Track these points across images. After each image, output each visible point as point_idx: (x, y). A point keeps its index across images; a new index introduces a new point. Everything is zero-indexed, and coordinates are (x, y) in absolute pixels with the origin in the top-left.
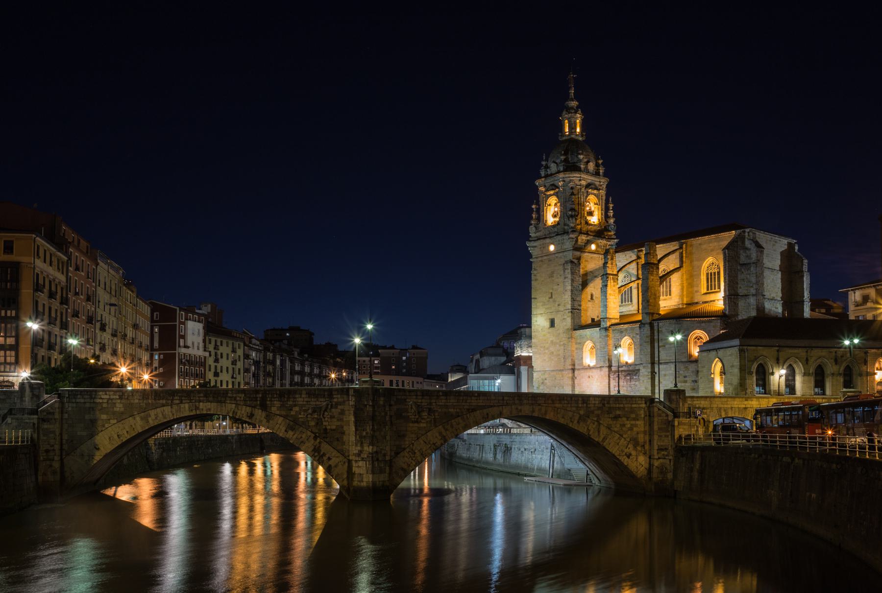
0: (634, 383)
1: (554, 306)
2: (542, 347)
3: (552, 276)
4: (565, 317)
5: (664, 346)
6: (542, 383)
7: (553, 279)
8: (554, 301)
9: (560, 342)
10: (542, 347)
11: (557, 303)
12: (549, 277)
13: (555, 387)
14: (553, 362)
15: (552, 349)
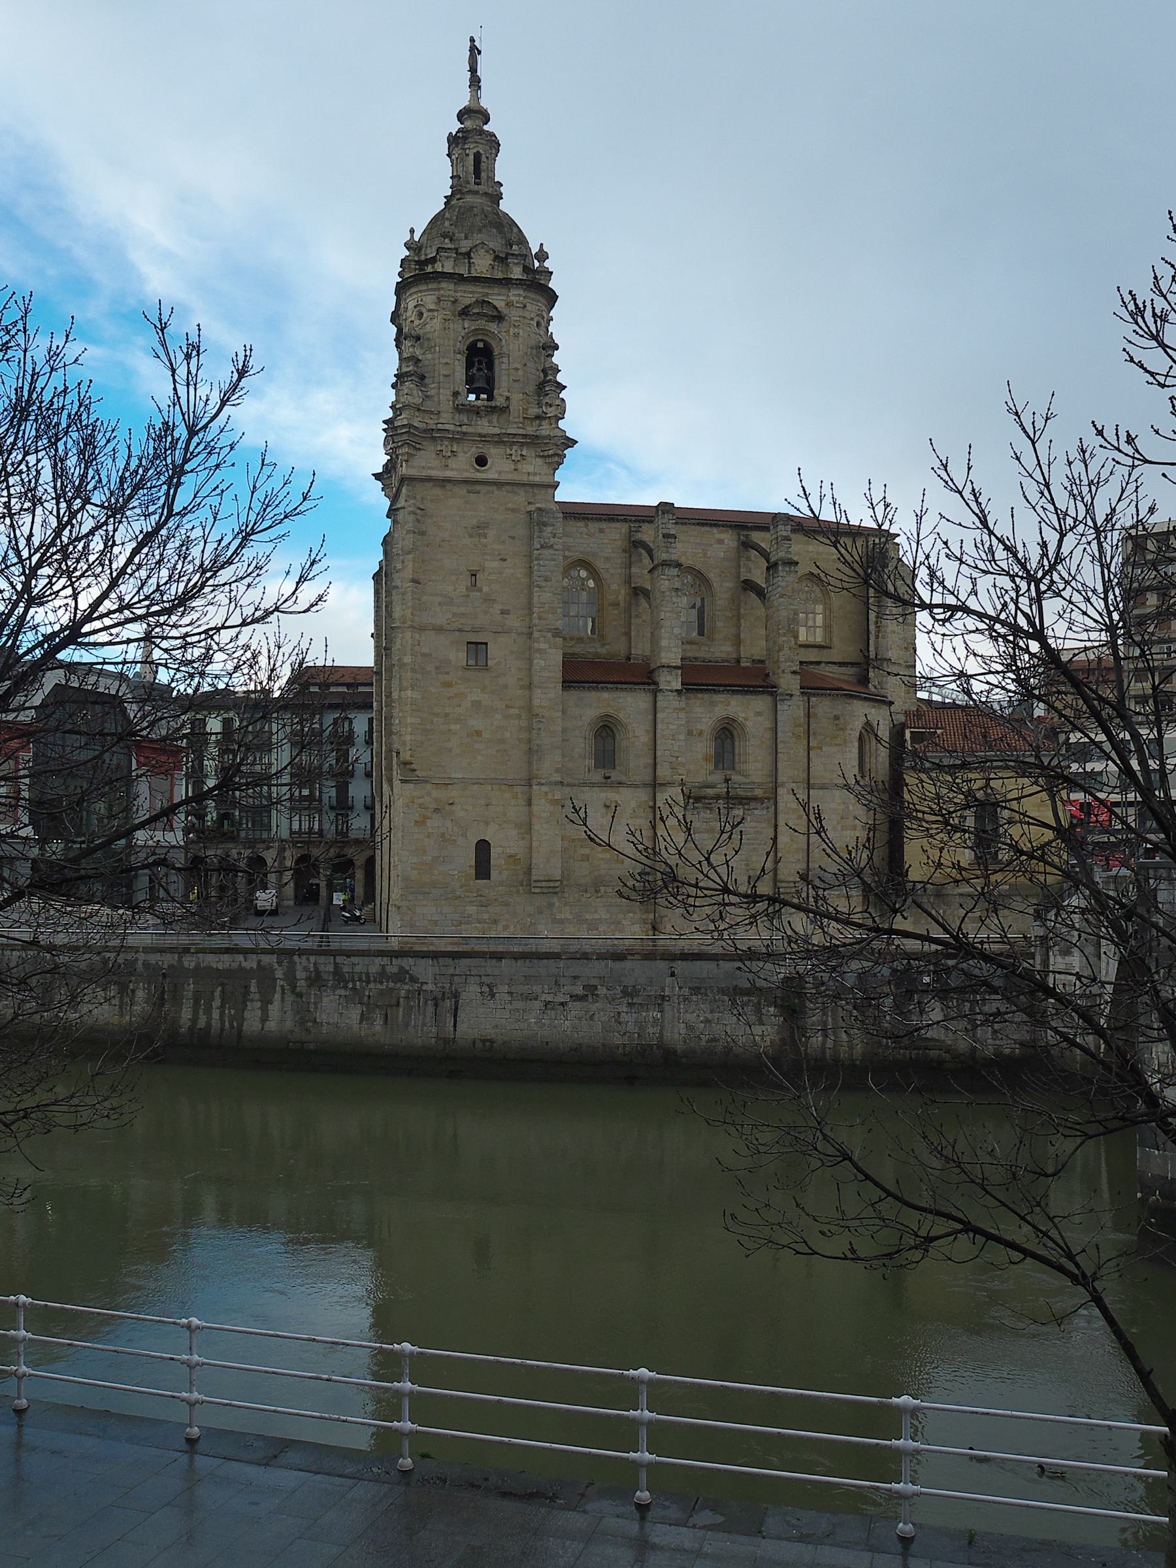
0: (753, 824)
1: (486, 613)
2: (437, 715)
3: (479, 535)
4: (543, 646)
5: (821, 748)
6: (436, 810)
7: (484, 540)
8: (488, 600)
9: (507, 706)
10: (437, 715)
11: (496, 609)
12: (471, 536)
13: (487, 823)
14: (479, 758)
15: (476, 723)
